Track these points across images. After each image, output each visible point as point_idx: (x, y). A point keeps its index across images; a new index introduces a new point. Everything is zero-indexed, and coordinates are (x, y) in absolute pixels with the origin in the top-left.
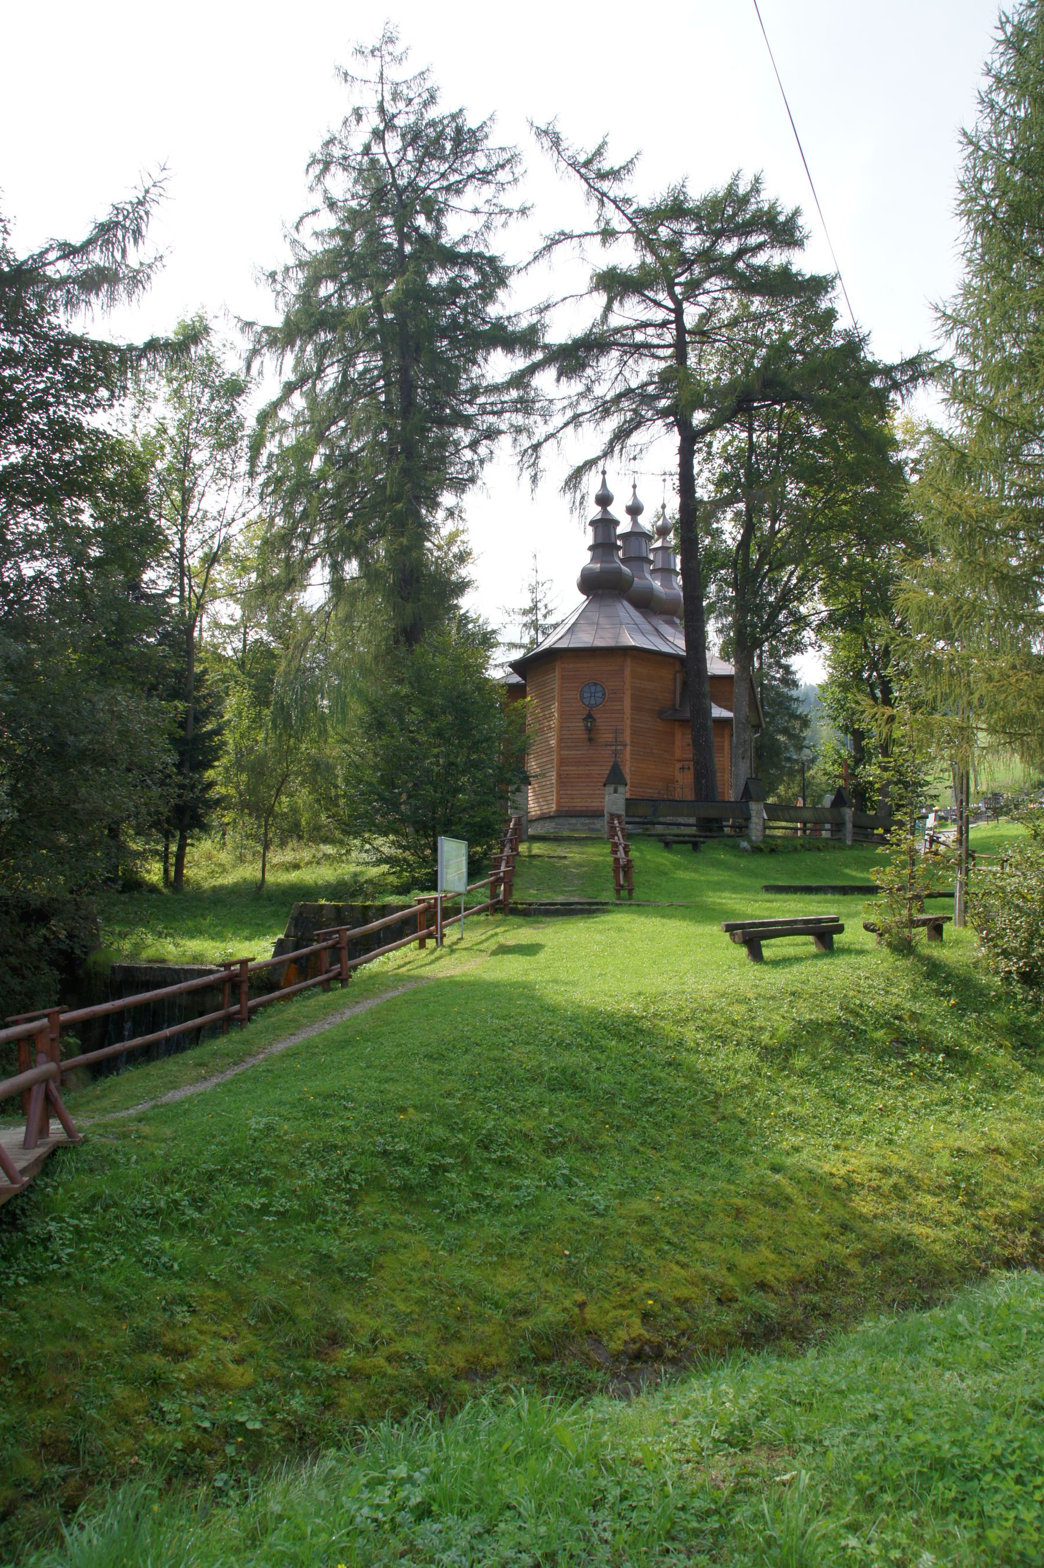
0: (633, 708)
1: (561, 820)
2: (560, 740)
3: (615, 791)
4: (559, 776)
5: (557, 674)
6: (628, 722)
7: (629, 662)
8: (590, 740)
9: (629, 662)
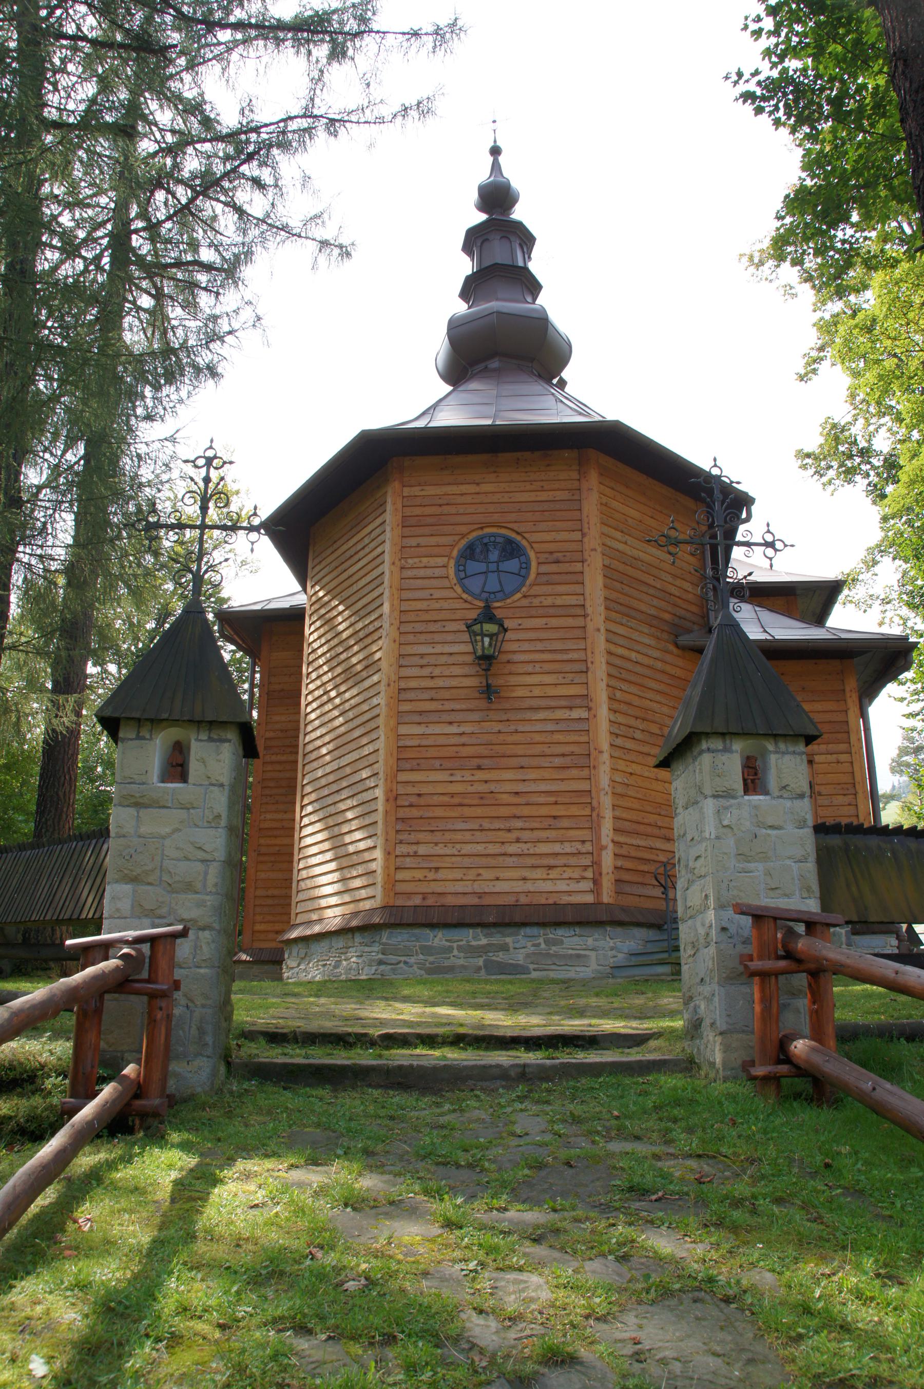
0: (610, 604)
1: (400, 938)
2: (401, 693)
3: (753, 779)
4: (393, 798)
5: (391, 516)
6: (600, 643)
7: (593, 478)
8: (489, 692)
9: (593, 478)
